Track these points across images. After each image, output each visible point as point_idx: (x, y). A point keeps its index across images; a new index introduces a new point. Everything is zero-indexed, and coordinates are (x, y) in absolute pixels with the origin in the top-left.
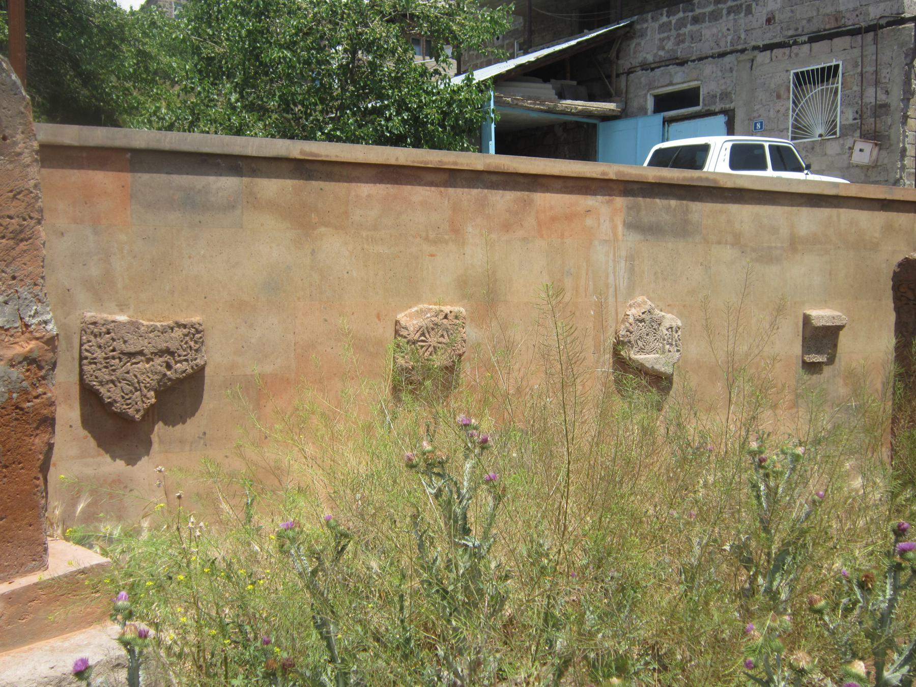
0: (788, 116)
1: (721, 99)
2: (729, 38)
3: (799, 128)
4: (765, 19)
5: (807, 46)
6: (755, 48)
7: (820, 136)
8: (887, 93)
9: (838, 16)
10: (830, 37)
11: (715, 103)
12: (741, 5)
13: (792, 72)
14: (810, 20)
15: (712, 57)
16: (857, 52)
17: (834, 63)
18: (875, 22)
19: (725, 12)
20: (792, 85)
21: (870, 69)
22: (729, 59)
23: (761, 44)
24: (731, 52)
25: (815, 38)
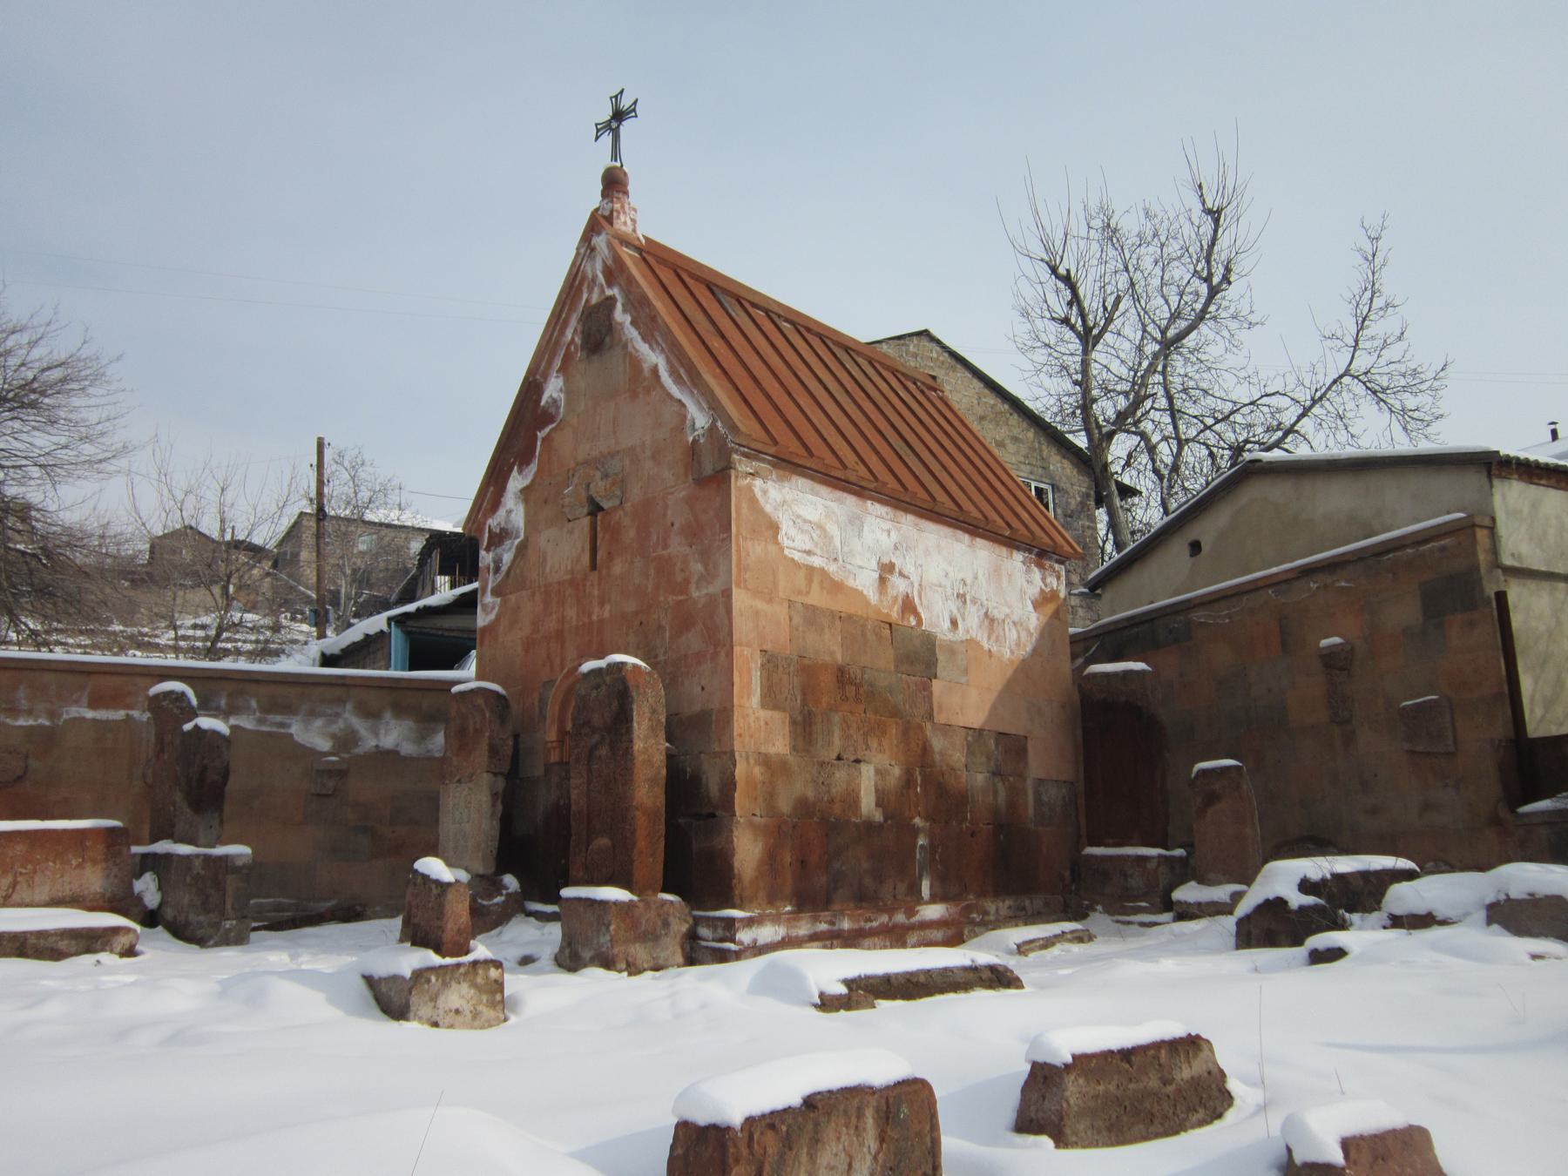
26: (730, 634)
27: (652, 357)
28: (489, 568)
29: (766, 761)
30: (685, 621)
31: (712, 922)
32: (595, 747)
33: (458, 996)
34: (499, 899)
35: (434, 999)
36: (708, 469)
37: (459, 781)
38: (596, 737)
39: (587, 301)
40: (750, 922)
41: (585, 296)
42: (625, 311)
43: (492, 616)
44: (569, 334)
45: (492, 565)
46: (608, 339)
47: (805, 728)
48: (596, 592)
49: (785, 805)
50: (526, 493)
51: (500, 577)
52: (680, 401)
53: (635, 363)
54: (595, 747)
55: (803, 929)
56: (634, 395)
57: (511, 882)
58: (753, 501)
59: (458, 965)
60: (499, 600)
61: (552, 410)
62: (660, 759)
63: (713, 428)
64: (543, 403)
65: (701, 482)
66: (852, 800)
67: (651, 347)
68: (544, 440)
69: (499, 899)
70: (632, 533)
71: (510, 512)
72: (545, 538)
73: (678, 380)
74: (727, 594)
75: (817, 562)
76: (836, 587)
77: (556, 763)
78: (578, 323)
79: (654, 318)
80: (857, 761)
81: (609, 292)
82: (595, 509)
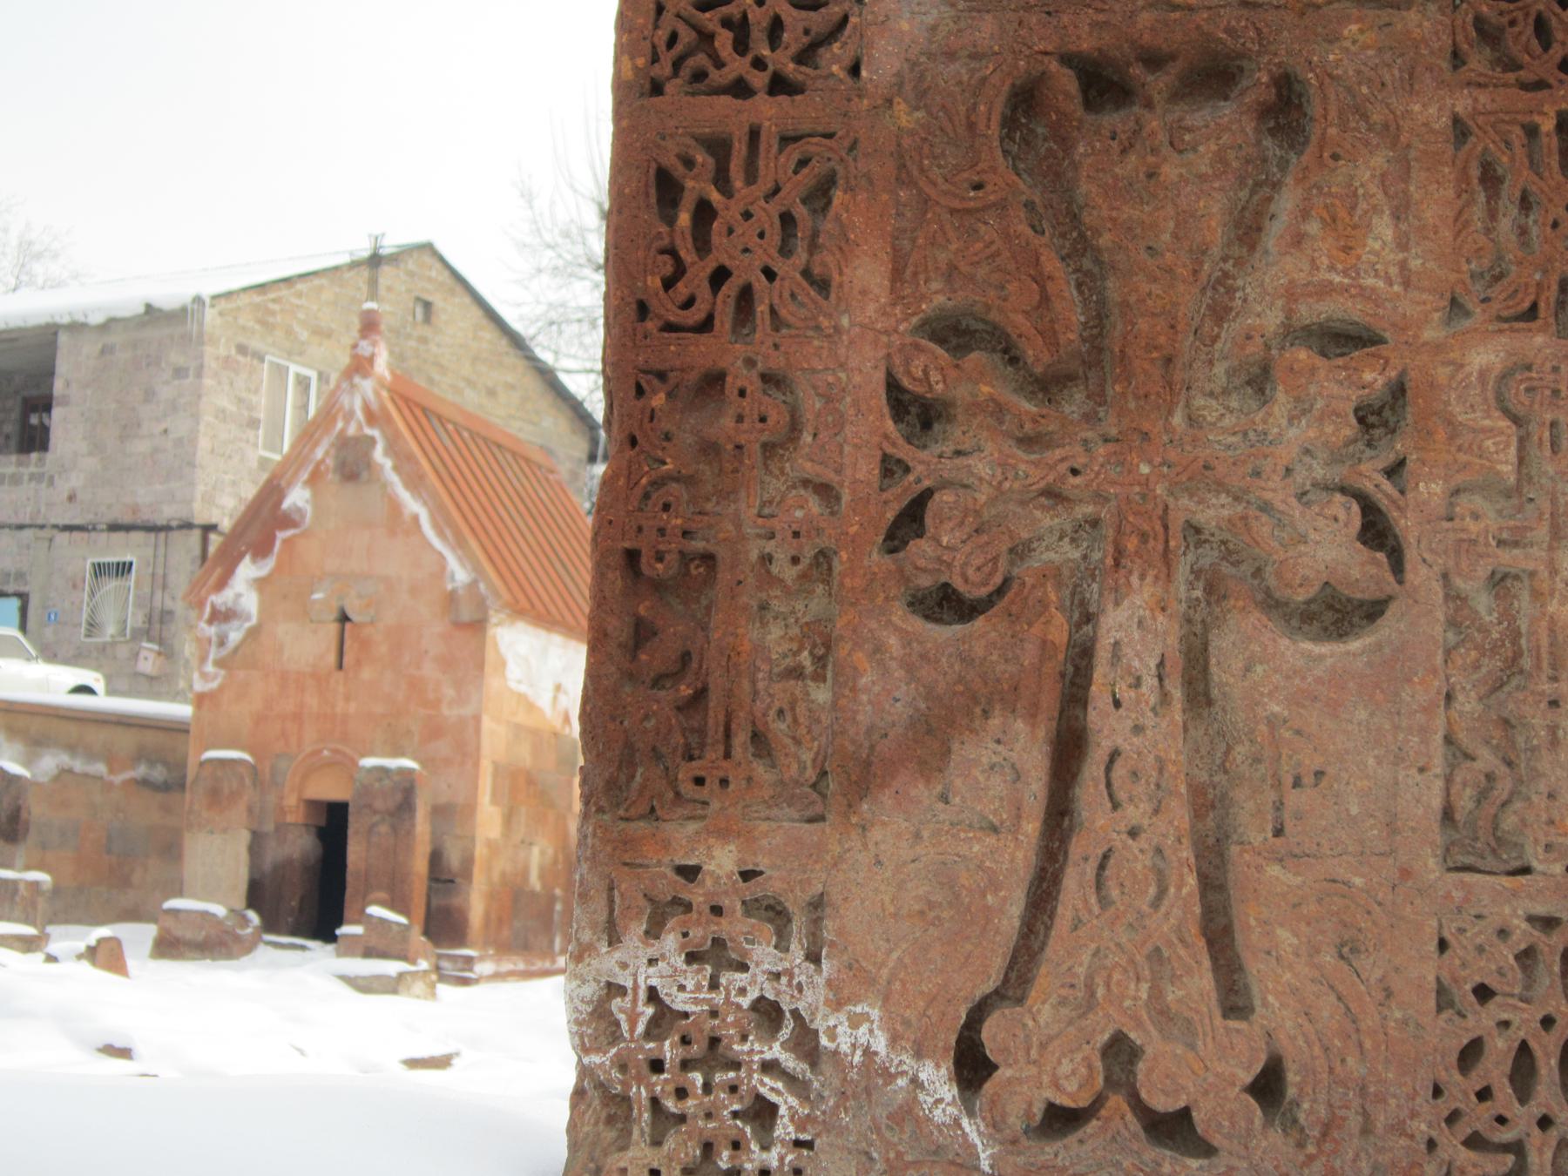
0: (81, 609)
1: (16, 579)
2: (29, 509)
3: (91, 625)
4: (66, 495)
5: (104, 536)
6: (55, 527)
7: (112, 636)
8: (173, 598)
9: (135, 510)
10: (128, 528)
11: (8, 582)
12: (43, 474)
13: (89, 562)
14: (110, 507)
15: (10, 527)
16: (150, 552)
17: (128, 558)
18: (165, 523)
19: (26, 478)
20: (88, 576)
21: (160, 571)
22: (27, 533)
23: (61, 521)
24: (30, 526)
25: (114, 527)
26: (478, 748)
27: (412, 505)
28: (210, 641)
29: (490, 844)
30: (434, 731)
31: (450, 957)
32: (374, 825)
33: (419, 987)
34: (249, 931)
35: (409, 989)
36: (466, 615)
37: (212, 833)
38: (376, 818)
39: (343, 431)
40: (482, 959)
41: (340, 425)
42: (387, 453)
43: (214, 685)
44: (319, 453)
45: (214, 639)
46: (365, 475)
47: (508, 820)
48: (341, 689)
49: (496, 876)
50: (261, 584)
51: (224, 652)
52: (440, 554)
53: (395, 507)
54: (374, 825)
55: (507, 966)
56: (392, 533)
57: (253, 917)
58: (496, 645)
59: (417, 972)
60: (223, 672)
61: (296, 517)
62: (427, 837)
63: (473, 585)
64: (286, 505)
65: (459, 625)
66: (525, 873)
67: (413, 496)
68: (286, 542)
69: (249, 931)
70: (384, 649)
71: (239, 596)
72: (284, 630)
73: (441, 533)
74: (477, 719)
75: (523, 688)
76: (531, 707)
77: (290, 824)
78: (333, 445)
79: (422, 477)
80: (531, 844)
81: (369, 431)
82: (344, 618)
